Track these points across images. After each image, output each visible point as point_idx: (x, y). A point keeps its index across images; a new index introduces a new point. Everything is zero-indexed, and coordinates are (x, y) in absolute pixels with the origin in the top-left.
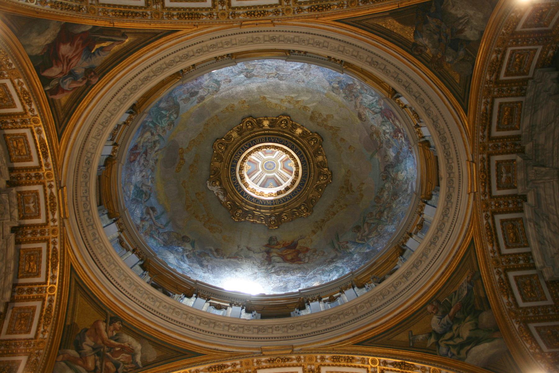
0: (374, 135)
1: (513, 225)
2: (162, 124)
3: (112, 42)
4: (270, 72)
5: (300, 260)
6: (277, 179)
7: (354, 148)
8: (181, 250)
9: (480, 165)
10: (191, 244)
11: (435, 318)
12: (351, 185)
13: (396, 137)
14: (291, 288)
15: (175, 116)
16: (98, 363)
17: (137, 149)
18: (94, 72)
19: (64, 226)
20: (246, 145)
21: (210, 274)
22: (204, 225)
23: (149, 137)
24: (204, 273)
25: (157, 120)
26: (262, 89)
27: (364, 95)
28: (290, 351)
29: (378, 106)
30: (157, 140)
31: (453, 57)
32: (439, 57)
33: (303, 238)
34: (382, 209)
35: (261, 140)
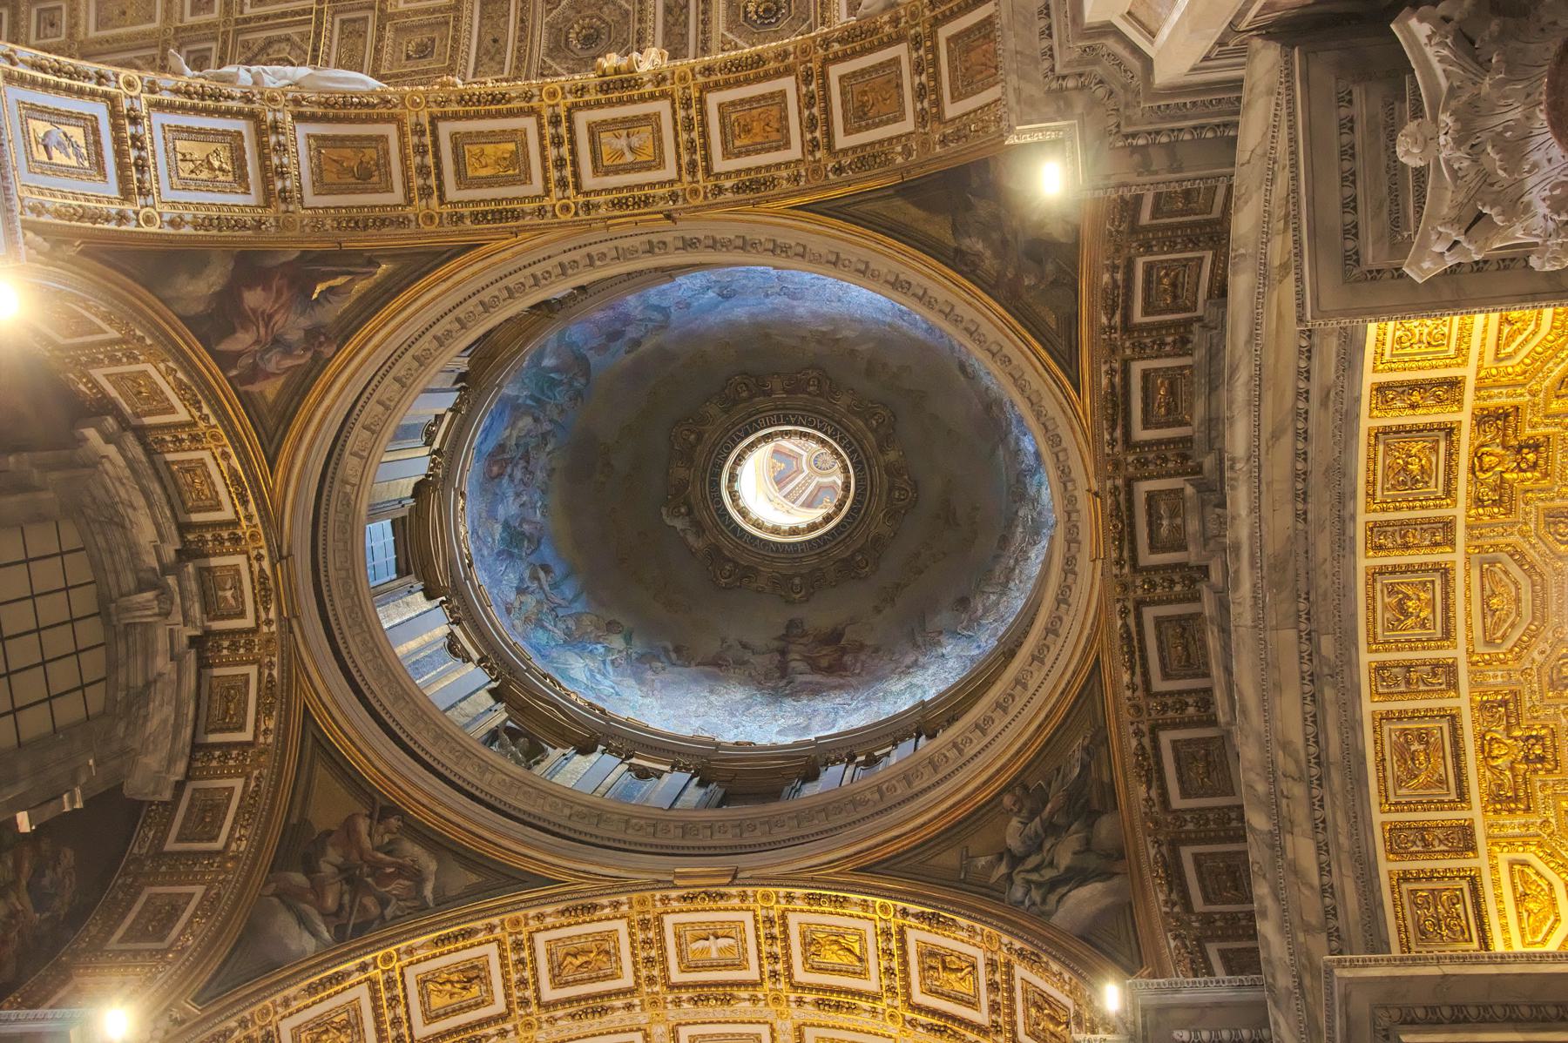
1: (1184, 629)
2: (555, 398)
3: (349, 277)
8: (602, 650)
9: (1109, 502)
10: (625, 638)
11: (1015, 822)
16: (346, 898)
17: (504, 452)
19: (291, 631)
28: (728, 880)
32: (1010, 276)
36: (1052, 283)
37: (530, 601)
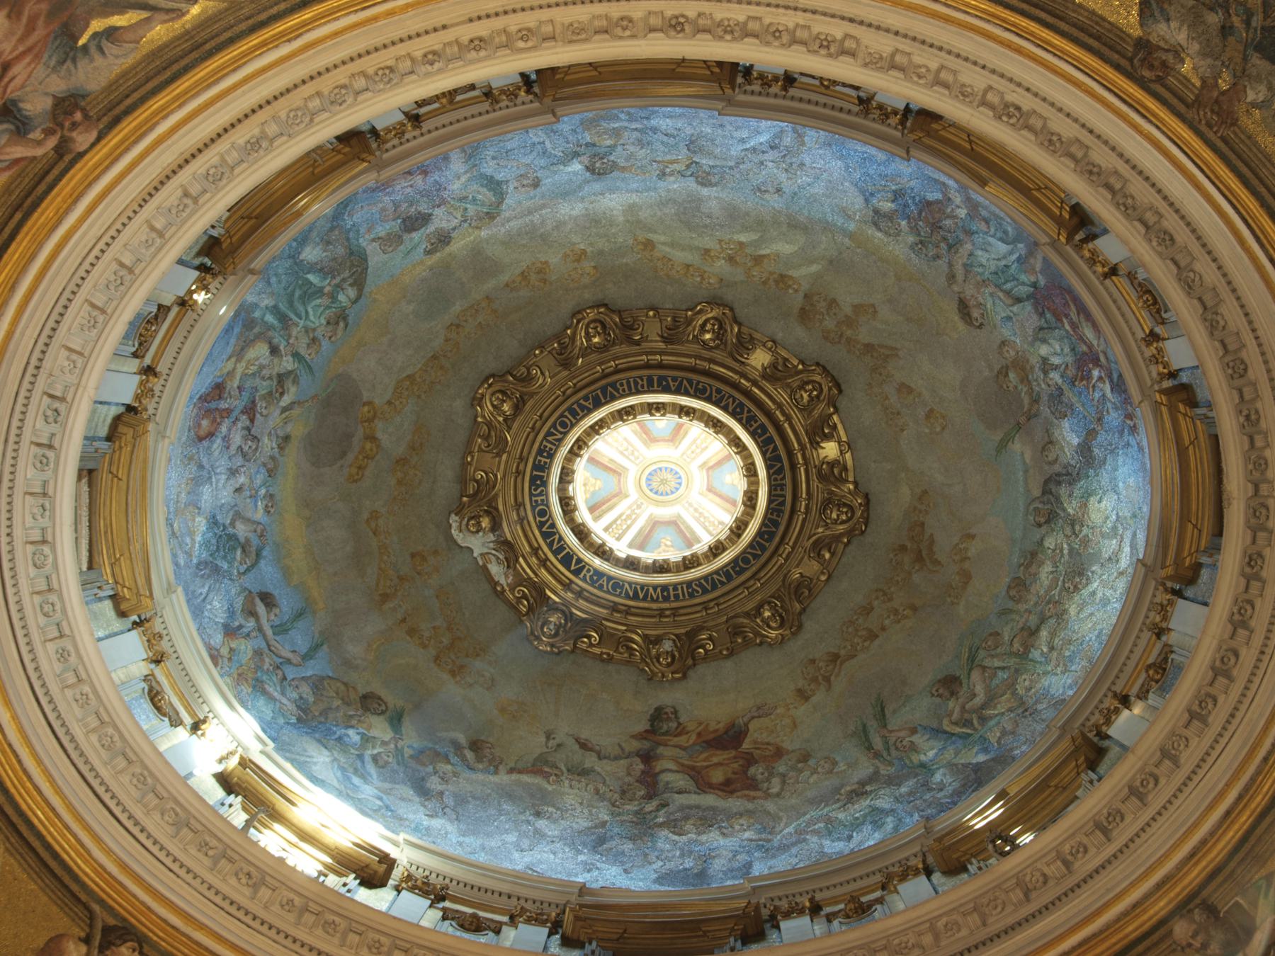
0: (1012, 375)
4: (669, 157)
5: (752, 785)
6: (688, 527)
7: (943, 417)
12: (932, 542)
13: (1082, 380)
14: (721, 875)
15: (352, 293)
18: (83, 110)
21: (450, 820)
22: (437, 659)
23: (262, 361)
24: (431, 816)
25: (291, 304)
26: (644, 215)
27: (979, 239)
29: (1023, 277)
30: (290, 372)
33: (767, 715)
34: (1033, 620)
35: (636, 383)
37: (245, 648)
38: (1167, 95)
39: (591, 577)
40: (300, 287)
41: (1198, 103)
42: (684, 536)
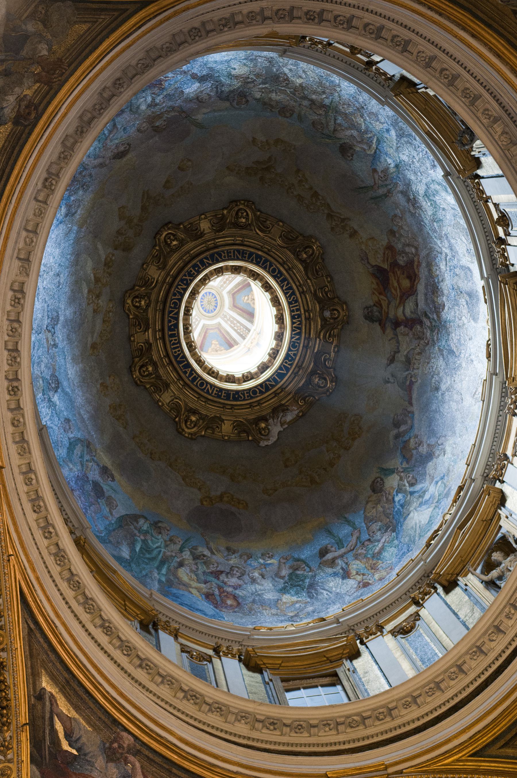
0: (157, 124)
3: (56, 718)
5: (410, 263)
6: (236, 286)
10: (386, 475)
12: (258, 162)
13: (161, 84)
15: (141, 521)
20: (185, 373)
22: (347, 449)
23: (188, 572)
30: (191, 553)
31: (40, 42)
34: (306, 103)
35: (174, 344)
36: (45, 26)
37: (355, 565)
38: (45, 102)
39: (289, 361)
40: (144, 554)
41: (49, 83)
42: (241, 289)
